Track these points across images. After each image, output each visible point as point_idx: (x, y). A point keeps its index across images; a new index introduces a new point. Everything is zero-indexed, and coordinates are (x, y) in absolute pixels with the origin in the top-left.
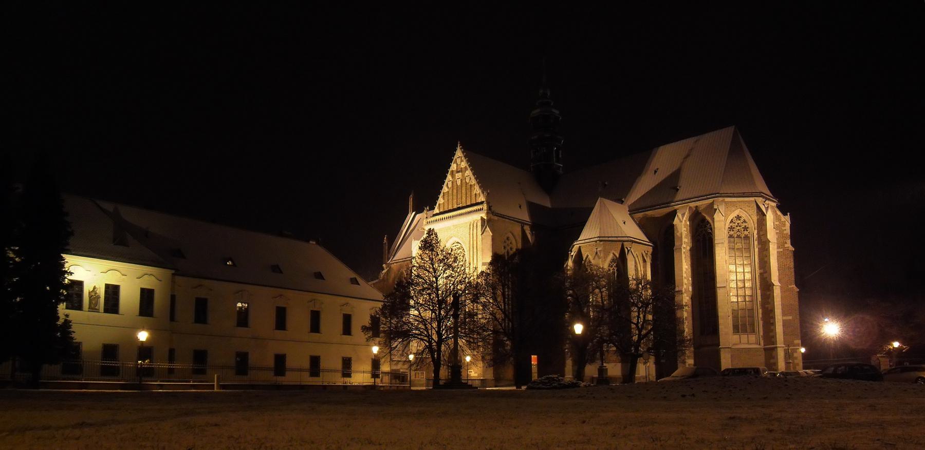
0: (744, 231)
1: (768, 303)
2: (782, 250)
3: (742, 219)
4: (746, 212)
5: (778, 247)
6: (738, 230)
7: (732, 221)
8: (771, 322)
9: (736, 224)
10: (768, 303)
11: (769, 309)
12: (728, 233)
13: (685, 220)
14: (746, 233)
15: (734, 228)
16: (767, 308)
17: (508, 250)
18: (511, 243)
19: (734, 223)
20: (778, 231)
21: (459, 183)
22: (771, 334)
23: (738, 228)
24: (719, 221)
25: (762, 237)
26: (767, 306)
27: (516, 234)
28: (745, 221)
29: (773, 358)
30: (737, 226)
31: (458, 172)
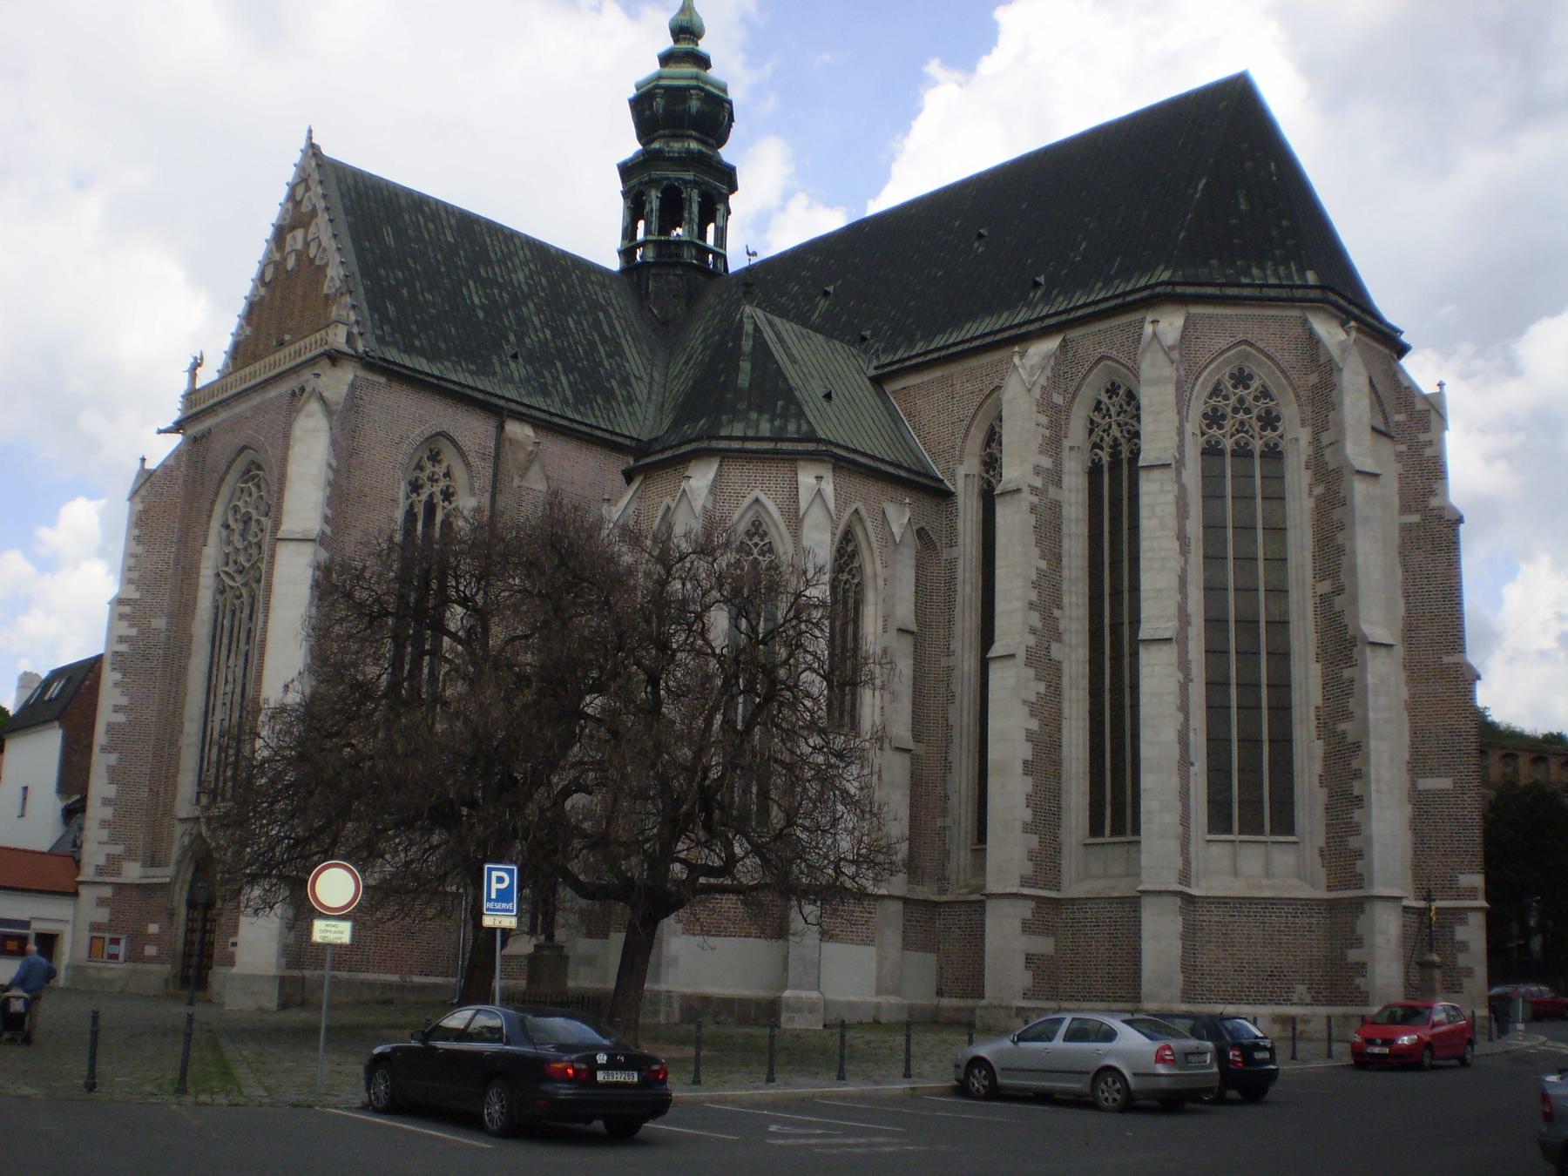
0: (1263, 428)
1: (1347, 715)
2: (1416, 518)
3: (1255, 384)
4: (1269, 357)
5: (1405, 509)
6: (1242, 423)
7: (1216, 391)
8: (1356, 792)
9: (1233, 399)
10: (1347, 715)
11: (1350, 740)
12: (1203, 434)
13: (1043, 387)
14: (1268, 433)
15: (1223, 417)
16: (1344, 732)
17: (431, 496)
18: (447, 475)
19: (1226, 398)
20: (1403, 448)
21: (291, 263)
22: (1354, 842)
23: (1239, 416)
24: (1157, 382)
25: (1327, 452)
26: (1342, 727)
27: (465, 443)
28: (1265, 393)
29: (1358, 942)
30: (1235, 410)
31: (293, 228)
